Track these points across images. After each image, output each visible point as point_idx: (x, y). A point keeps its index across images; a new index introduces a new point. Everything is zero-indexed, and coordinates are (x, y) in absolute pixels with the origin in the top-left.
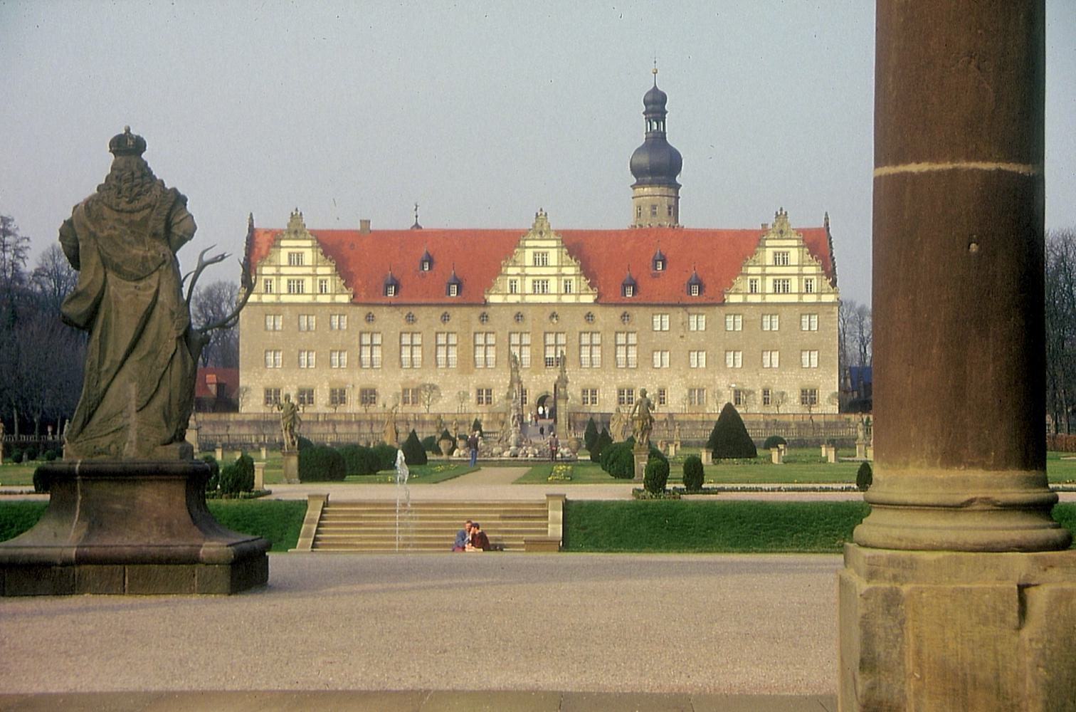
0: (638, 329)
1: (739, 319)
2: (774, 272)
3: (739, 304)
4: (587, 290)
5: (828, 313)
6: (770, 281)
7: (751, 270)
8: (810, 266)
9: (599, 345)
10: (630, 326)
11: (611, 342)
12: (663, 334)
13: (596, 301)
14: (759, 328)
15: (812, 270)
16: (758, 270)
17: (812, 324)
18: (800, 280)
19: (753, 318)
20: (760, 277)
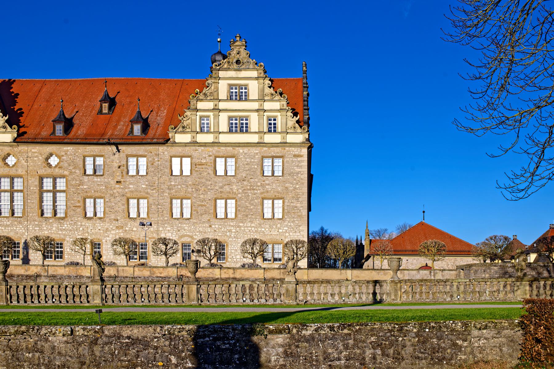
0: (66, 173)
1: (187, 162)
2: (229, 108)
3: (186, 145)
4: (4, 127)
5: (295, 156)
6: (224, 118)
7: (201, 105)
8: (272, 100)
9: (21, 191)
10: (57, 170)
11: (35, 189)
12: (96, 179)
13: (15, 140)
14: (211, 172)
15: (276, 105)
16: (210, 105)
17: (276, 169)
18: (260, 118)
19: (204, 161)
20: (211, 114)
